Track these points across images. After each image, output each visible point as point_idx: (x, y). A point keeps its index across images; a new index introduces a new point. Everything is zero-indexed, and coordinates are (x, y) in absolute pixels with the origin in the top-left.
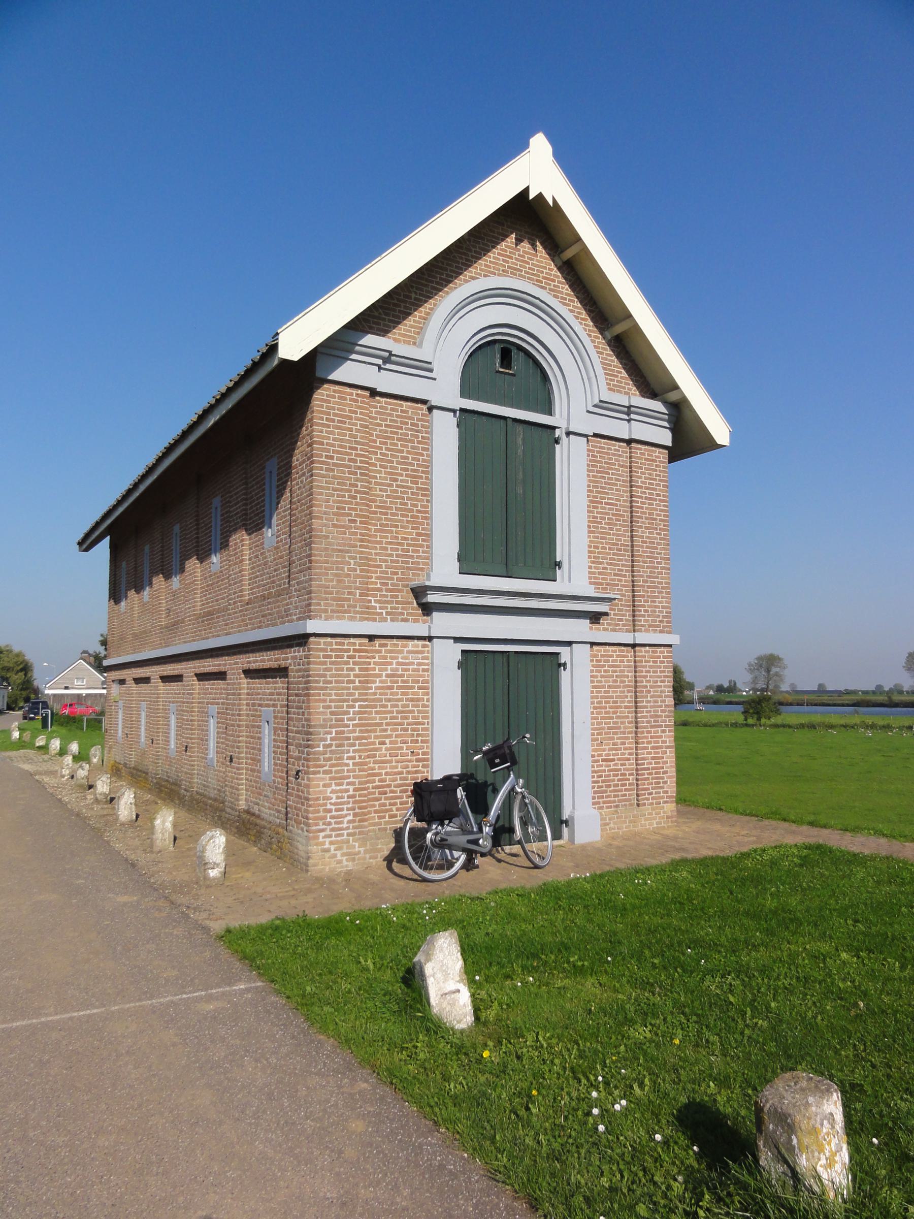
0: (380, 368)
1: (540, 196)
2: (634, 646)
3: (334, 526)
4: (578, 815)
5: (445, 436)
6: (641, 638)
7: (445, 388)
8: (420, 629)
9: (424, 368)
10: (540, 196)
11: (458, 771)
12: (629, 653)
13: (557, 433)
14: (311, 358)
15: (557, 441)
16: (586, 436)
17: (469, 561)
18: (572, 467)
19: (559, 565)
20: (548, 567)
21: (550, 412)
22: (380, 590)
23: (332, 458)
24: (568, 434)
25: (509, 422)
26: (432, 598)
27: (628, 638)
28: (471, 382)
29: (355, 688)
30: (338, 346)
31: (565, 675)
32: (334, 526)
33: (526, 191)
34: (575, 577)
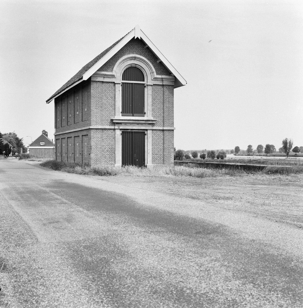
0: (104, 77)
1: (137, 38)
2: (163, 130)
3: (95, 108)
4: (148, 165)
5: (119, 89)
6: (165, 128)
7: (119, 79)
8: (113, 127)
9: (113, 76)
10: (137, 38)
11: (175, 89)
12: (161, 133)
13: (145, 85)
14: (90, 78)
15: (145, 87)
16: (152, 85)
17: (124, 112)
18: (148, 92)
19: (145, 113)
20: (142, 113)
21: (144, 81)
22: (104, 120)
23: (94, 96)
24: (147, 85)
25: (133, 84)
26: (114, 121)
27: (161, 128)
28: (125, 77)
29: (100, 139)
30: (95, 74)
31: (146, 136)
32: (95, 108)
33: (134, 37)
34: (149, 116)
